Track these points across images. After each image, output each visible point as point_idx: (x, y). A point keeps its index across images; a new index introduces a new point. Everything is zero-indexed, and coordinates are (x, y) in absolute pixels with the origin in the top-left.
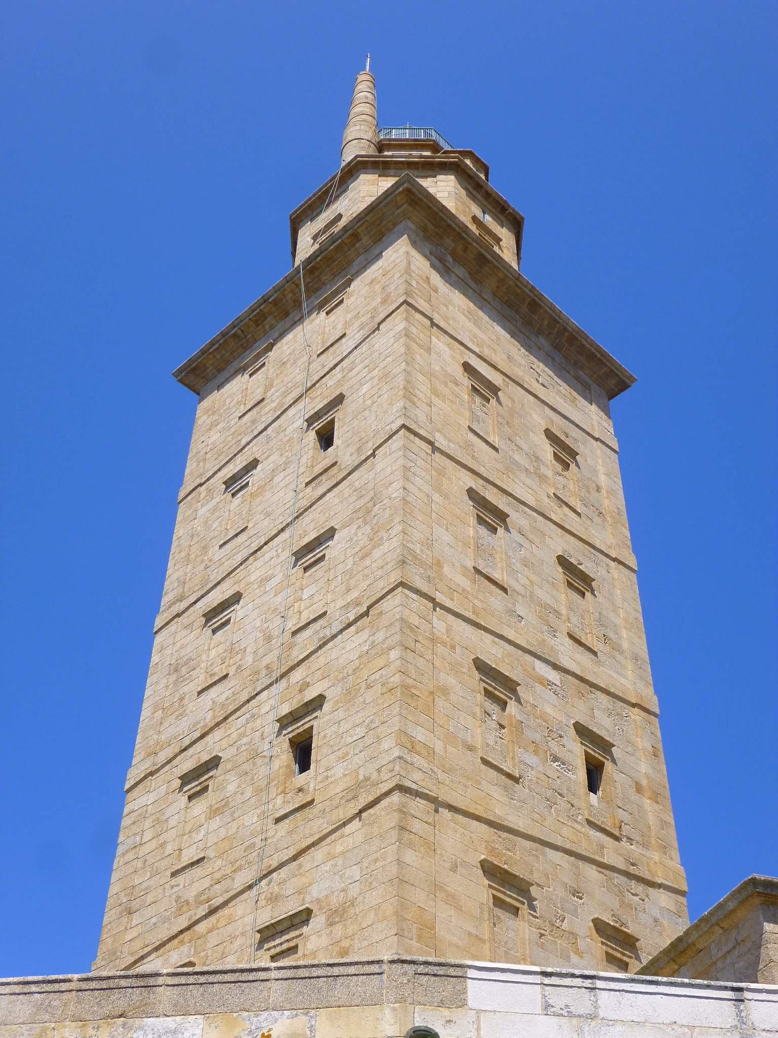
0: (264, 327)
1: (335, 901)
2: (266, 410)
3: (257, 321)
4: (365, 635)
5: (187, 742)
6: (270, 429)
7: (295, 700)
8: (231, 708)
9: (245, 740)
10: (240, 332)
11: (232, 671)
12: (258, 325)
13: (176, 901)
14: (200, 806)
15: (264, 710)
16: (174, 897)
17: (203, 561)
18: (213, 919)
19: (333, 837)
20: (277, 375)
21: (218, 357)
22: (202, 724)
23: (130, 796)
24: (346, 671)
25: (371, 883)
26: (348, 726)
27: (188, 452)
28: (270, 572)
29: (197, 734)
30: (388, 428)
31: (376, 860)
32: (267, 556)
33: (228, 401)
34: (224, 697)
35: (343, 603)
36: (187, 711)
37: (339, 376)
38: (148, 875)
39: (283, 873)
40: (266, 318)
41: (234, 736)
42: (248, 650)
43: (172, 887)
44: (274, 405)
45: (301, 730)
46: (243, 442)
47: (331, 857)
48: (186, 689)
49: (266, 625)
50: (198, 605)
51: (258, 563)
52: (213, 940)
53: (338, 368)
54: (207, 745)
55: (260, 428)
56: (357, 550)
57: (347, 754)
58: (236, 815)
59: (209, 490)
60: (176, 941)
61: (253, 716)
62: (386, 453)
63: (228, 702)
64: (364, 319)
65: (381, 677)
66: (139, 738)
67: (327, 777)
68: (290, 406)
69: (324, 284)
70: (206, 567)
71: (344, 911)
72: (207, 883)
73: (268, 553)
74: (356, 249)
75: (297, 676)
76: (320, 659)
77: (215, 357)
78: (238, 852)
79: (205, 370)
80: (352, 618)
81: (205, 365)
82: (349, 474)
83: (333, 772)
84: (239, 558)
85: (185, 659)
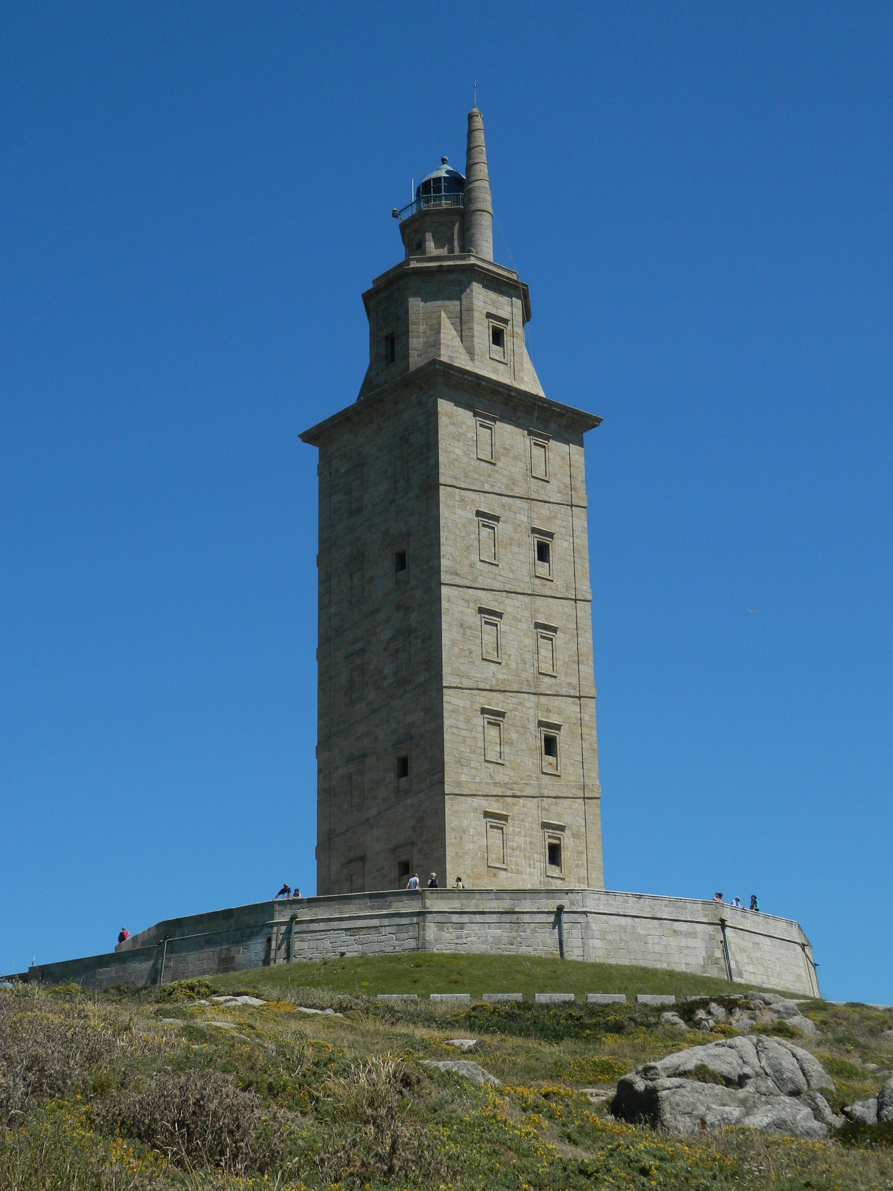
8: (508, 688)
11: (504, 663)
32: (517, 603)
44: (504, 480)
48: (473, 648)
51: (510, 601)
72: (507, 779)
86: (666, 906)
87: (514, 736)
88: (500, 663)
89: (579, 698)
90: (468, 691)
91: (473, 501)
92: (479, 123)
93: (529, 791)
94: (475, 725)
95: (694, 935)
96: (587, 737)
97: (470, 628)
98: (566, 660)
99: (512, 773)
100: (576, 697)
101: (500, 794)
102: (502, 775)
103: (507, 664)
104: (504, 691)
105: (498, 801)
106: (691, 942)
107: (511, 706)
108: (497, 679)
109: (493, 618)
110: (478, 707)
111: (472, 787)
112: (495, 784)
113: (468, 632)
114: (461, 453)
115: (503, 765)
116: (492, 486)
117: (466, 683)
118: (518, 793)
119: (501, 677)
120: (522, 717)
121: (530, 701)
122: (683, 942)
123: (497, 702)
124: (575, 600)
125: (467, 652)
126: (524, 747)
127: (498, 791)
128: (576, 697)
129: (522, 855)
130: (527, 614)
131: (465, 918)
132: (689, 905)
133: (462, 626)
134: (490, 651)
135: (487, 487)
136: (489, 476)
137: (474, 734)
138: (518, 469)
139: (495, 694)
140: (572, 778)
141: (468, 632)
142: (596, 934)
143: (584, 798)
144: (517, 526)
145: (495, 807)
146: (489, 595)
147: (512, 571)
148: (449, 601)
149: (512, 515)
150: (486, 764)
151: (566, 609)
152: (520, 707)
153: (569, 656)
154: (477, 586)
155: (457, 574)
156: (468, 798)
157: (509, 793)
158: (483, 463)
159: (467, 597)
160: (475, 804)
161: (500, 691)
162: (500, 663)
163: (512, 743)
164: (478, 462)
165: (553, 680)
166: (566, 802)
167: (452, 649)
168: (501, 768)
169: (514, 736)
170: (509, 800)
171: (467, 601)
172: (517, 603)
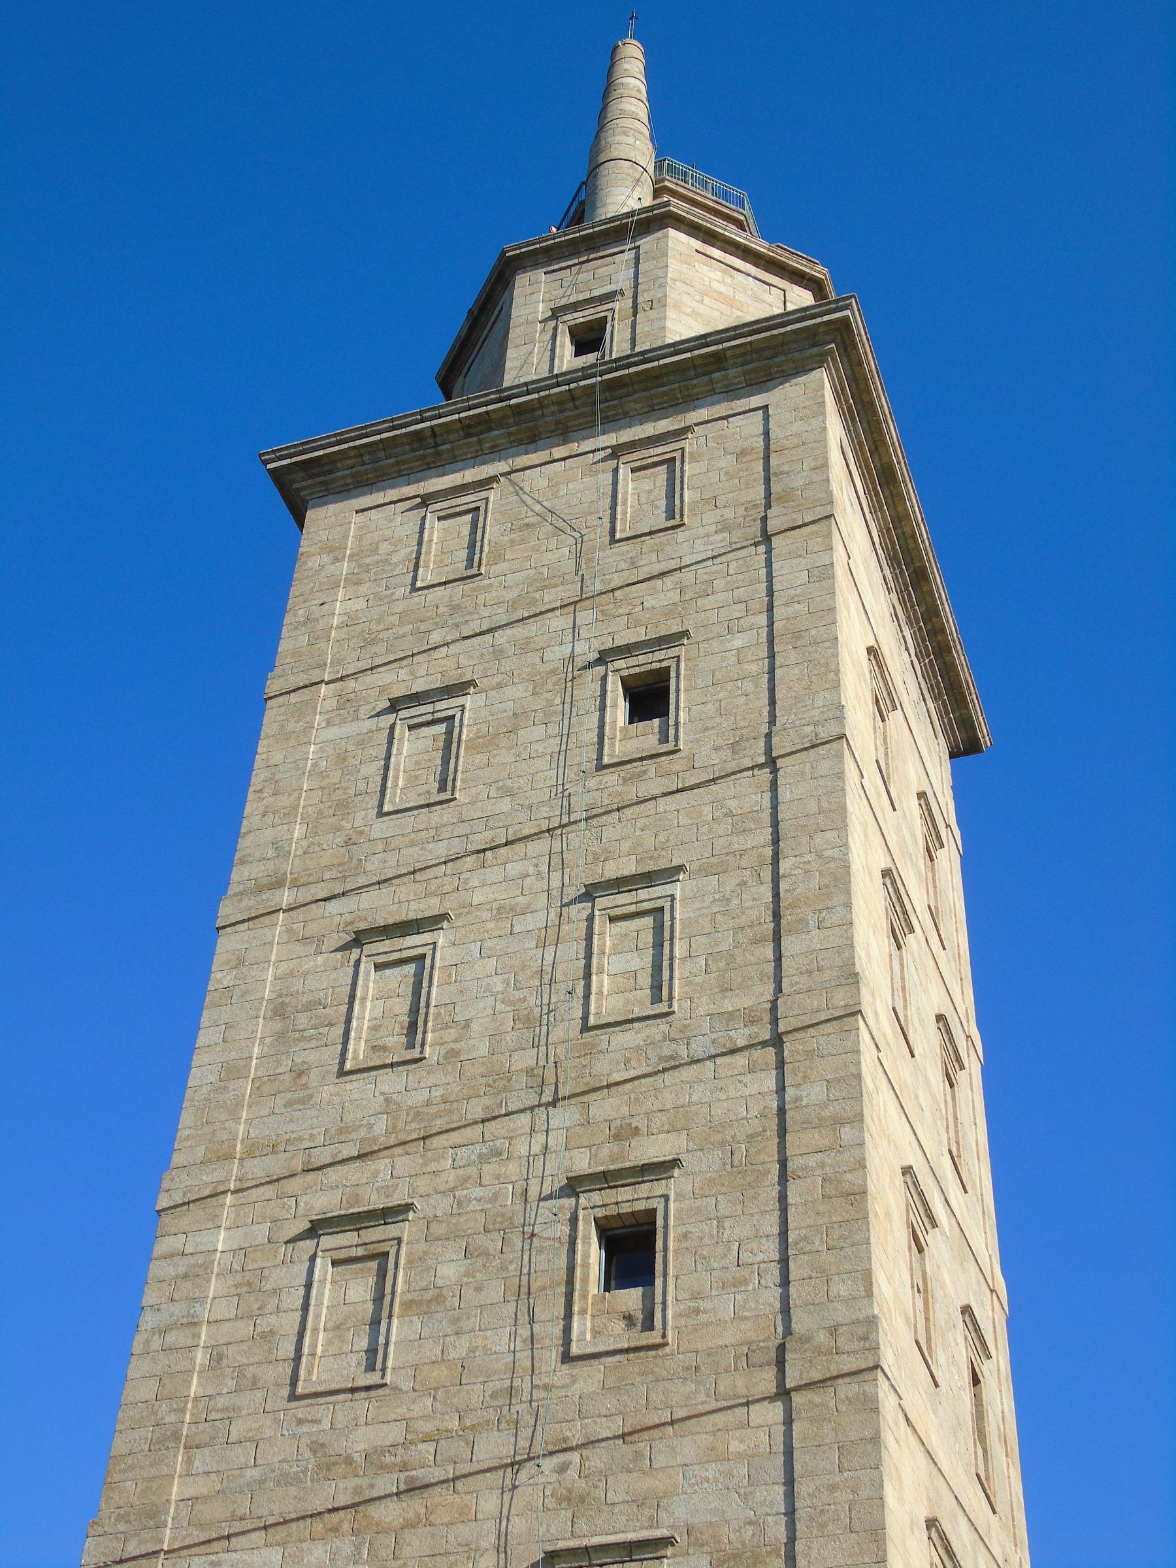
0: (480, 442)
2: (491, 597)
3: (469, 426)
6: (501, 637)
7: (605, 1152)
8: (440, 1123)
9: (477, 1192)
10: (428, 433)
12: (469, 436)
13: (314, 1452)
16: (305, 1441)
17: (339, 829)
18: (415, 1506)
20: (512, 542)
21: (367, 458)
22: (363, 1133)
23: (166, 1219)
25: (824, 1525)
27: (283, 611)
32: (514, 869)
33: (384, 548)
34: (420, 1097)
35: (713, 1009)
36: (316, 1099)
38: (231, 1384)
40: (490, 429)
41: (451, 1177)
42: (475, 1026)
43: (300, 1422)
44: (510, 595)
46: (436, 637)
47: (713, 1455)
48: (312, 1058)
49: (518, 995)
50: (333, 907)
51: (492, 875)
53: (669, 581)
54: (376, 1173)
55: (476, 626)
56: (743, 921)
57: (745, 1282)
58: (466, 1324)
59: (344, 701)
61: (496, 1152)
63: (433, 1110)
64: (729, 513)
65: (822, 1165)
66: (187, 1118)
67: (697, 1311)
69: (626, 415)
70: (349, 842)
72: (394, 1434)
73: (516, 863)
74: (711, 382)
75: (605, 1108)
77: (361, 455)
78: (475, 1393)
79: (330, 472)
80: (741, 1043)
81: (334, 462)
83: (708, 1305)
84: (441, 850)
85: (304, 999)
87: (450, 1271)
94: (277, 1292)
96: (812, 1161)
103: (452, 1054)
105: (336, 1529)
111: (215, 1511)
113: (302, 1020)
123: (373, 1185)
137: (264, 1324)
159: (314, 928)
163: (439, 1299)
166: (688, 1447)
169: (450, 1271)
172: (514, 869)
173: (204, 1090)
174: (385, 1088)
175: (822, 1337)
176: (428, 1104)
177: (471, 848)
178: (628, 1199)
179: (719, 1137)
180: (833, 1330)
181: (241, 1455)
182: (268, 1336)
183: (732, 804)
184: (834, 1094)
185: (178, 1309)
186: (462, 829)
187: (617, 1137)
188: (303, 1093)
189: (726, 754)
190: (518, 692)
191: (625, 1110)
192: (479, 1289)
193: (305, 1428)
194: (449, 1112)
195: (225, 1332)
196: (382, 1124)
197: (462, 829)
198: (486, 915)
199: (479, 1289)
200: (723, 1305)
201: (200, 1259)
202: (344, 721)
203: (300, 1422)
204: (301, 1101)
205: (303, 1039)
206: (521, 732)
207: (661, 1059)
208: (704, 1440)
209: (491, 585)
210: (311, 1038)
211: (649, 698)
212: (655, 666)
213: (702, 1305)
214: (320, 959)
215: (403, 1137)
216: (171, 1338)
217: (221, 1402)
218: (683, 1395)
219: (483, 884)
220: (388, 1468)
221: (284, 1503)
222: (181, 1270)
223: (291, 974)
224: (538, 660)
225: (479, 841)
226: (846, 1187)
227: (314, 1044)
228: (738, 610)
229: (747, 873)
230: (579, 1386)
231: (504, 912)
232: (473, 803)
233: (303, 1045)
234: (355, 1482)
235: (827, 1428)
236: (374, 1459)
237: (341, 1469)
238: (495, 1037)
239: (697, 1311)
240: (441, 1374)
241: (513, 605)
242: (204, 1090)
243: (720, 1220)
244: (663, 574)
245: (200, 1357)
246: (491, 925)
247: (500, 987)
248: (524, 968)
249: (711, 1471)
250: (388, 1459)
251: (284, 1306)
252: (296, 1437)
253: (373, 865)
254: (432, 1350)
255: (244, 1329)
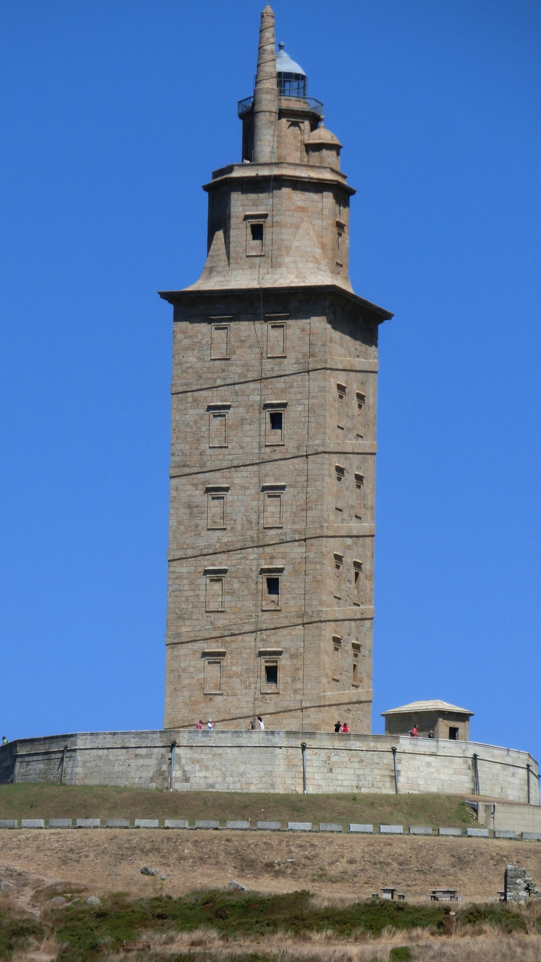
1: (292, 651)
4: (304, 550)
5: (205, 552)
6: (237, 387)
8: (231, 548)
9: (240, 567)
11: (229, 528)
14: (217, 586)
15: (251, 557)
19: (291, 628)
22: (214, 547)
24: (294, 561)
26: (296, 586)
28: (247, 485)
29: (211, 551)
30: (315, 447)
31: (311, 644)
32: (245, 474)
33: (200, 336)
36: (201, 535)
37: (283, 385)
39: (268, 632)
42: (238, 521)
43: (207, 617)
44: (239, 370)
45: (273, 577)
48: (199, 522)
50: (199, 476)
51: (239, 474)
52: (234, 645)
54: (218, 558)
56: (298, 504)
57: (296, 598)
60: (214, 640)
62: (313, 461)
65: (312, 573)
68: (251, 381)
70: (201, 454)
71: (297, 656)
72: (227, 622)
75: (268, 550)
76: (281, 548)
80: (297, 539)
82: (293, 458)
85: (195, 504)
86: (133, 738)
87: (236, 586)
88: (225, 529)
89: (305, 540)
90: (193, 559)
91: (205, 398)
92: (269, 21)
93: (247, 628)
94: (198, 585)
95: (149, 756)
96: (311, 572)
97: (197, 506)
98: (294, 510)
99: (232, 616)
100: (302, 540)
101: (219, 635)
102: (222, 621)
103: (232, 528)
104: (228, 551)
105: (217, 641)
106: (147, 761)
107: (234, 562)
108: (221, 543)
109: (219, 493)
110: (201, 569)
111: (192, 634)
112: (215, 629)
113: (195, 510)
114: (195, 360)
115: (224, 612)
116: (224, 379)
117: (190, 552)
118: (237, 632)
119: (225, 540)
120: (244, 569)
121: (252, 554)
122: (141, 762)
124: (307, 456)
125: (194, 527)
126: (246, 593)
127: (217, 634)
128: (302, 540)
129: (238, 680)
130: (255, 480)
131: (31, 759)
132: (150, 736)
133: (190, 507)
134: (218, 520)
135: (219, 382)
136: (223, 371)
137: (197, 592)
138: (252, 357)
139: (219, 555)
140: (293, 610)
141: (195, 510)
142: (80, 764)
143: (303, 624)
144: (249, 407)
145: (214, 647)
146: (218, 474)
147: (242, 448)
148: (177, 490)
149: (246, 398)
150: (207, 614)
151: (297, 466)
152: (243, 561)
153: (297, 506)
154: (206, 469)
155: (184, 466)
156: (189, 644)
157: (227, 633)
158: (217, 362)
159: (195, 481)
160: (196, 647)
161: (224, 552)
162: (225, 529)
163: (234, 592)
164: (212, 363)
165: (280, 531)
166: (285, 631)
167: (178, 528)
168: (221, 615)
169: (236, 586)
170: (228, 639)
171: (196, 485)
173: (174, 527)
174: (217, 535)
175: (311, 613)
176: (228, 542)
177: (233, 465)
178: (274, 575)
179: (292, 562)
180: (312, 612)
181: (195, 622)
182: (198, 596)
183: (297, 466)
184: (316, 556)
185: (176, 587)
186: (230, 457)
187: (270, 558)
188: (198, 532)
189: (296, 450)
190: (242, 410)
191: (272, 552)
192: (243, 591)
193: (209, 618)
194: (233, 545)
195: (188, 594)
196: (218, 545)
197: (230, 457)
198: (238, 487)
199: (243, 591)
200: (292, 603)
201: (179, 574)
202: (194, 408)
203: (207, 617)
204: (198, 535)
205: (196, 516)
206: (244, 426)
207: (280, 540)
208: (288, 631)
209: (232, 364)
210: (198, 517)
211: (276, 421)
212: (278, 412)
213: (288, 602)
214: (198, 492)
215: (223, 550)
216: (176, 593)
217: (189, 610)
218: (285, 622)
219: (237, 477)
220: (227, 630)
221: (207, 635)
222: (175, 576)
223: (191, 496)
224: (247, 399)
225: (235, 463)
226: (317, 580)
227: (199, 518)
228: (299, 396)
229: (300, 489)
230: (264, 616)
231: (243, 488)
232: (233, 448)
233: (196, 518)
234: (220, 632)
235: (310, 632)
236: (224, 628)
237: (217, 629)
238: (242, 525)
239: (287, 603)
240: (236, 610)
241: (240, 375)
242: (174, 527)
243: (292, 583)
244: (281, 376)
245: (183, 599)
246: (240, 491)
247: (243, 511)
248: (248, 506)
249: (289, 637)
250: (227, 628)
251: (201, 589)
252: (207, 620)
253: (208, 464)
254: (233, 604)
255: (191, 593)
